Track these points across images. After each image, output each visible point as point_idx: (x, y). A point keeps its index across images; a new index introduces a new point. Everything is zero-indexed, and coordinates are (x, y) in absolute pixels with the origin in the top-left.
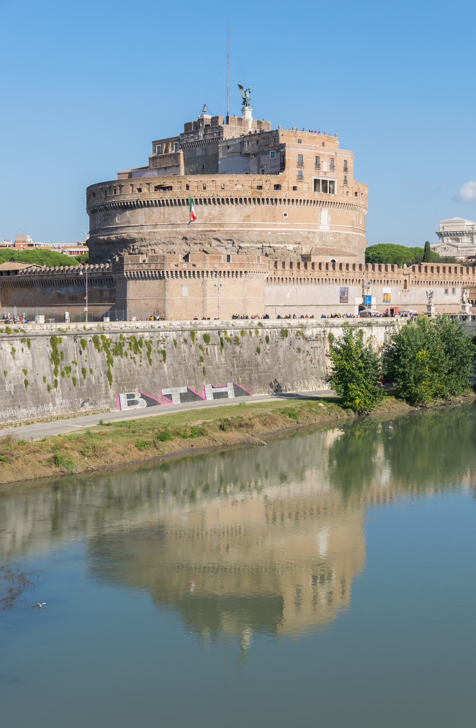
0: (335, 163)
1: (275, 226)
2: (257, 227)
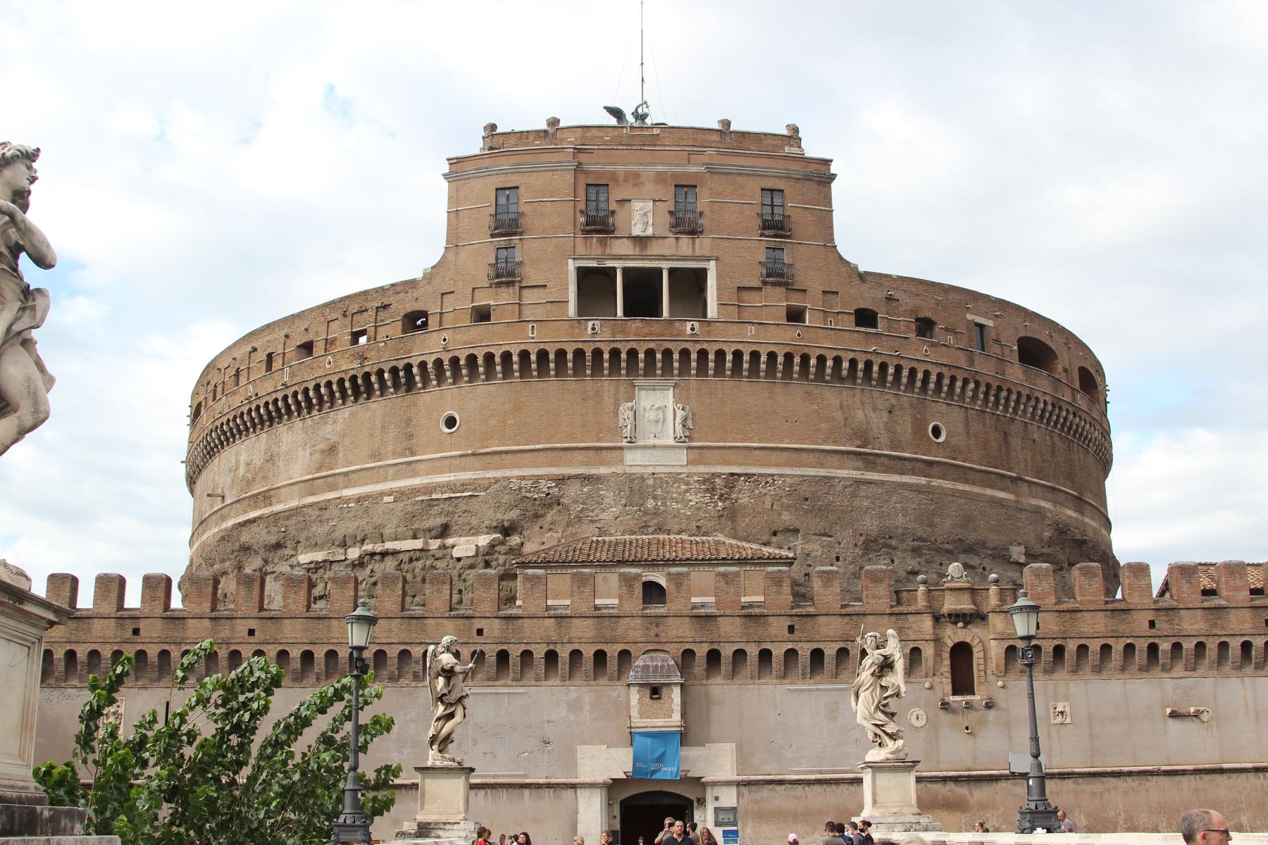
0: (703, 200)
1: (410, 468)
2: (355, 485)
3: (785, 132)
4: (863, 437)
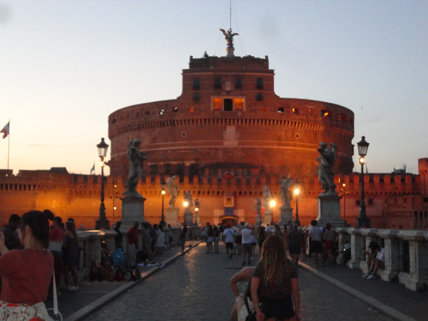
3: (264, 58)
4: (279, 139)
